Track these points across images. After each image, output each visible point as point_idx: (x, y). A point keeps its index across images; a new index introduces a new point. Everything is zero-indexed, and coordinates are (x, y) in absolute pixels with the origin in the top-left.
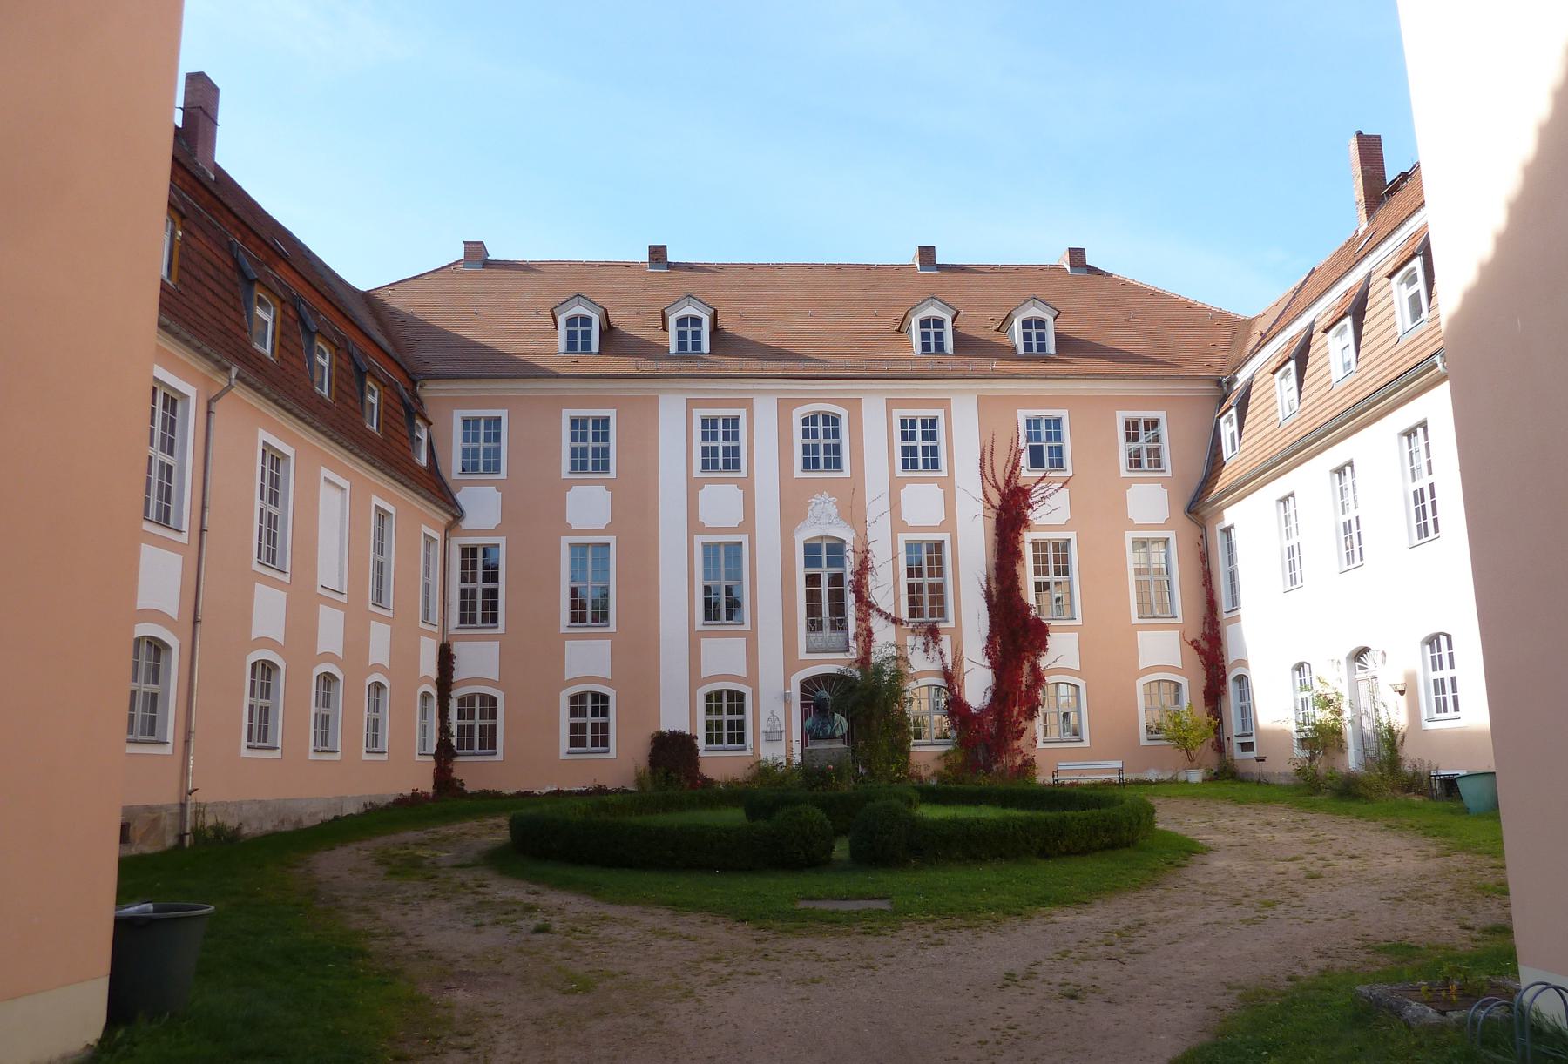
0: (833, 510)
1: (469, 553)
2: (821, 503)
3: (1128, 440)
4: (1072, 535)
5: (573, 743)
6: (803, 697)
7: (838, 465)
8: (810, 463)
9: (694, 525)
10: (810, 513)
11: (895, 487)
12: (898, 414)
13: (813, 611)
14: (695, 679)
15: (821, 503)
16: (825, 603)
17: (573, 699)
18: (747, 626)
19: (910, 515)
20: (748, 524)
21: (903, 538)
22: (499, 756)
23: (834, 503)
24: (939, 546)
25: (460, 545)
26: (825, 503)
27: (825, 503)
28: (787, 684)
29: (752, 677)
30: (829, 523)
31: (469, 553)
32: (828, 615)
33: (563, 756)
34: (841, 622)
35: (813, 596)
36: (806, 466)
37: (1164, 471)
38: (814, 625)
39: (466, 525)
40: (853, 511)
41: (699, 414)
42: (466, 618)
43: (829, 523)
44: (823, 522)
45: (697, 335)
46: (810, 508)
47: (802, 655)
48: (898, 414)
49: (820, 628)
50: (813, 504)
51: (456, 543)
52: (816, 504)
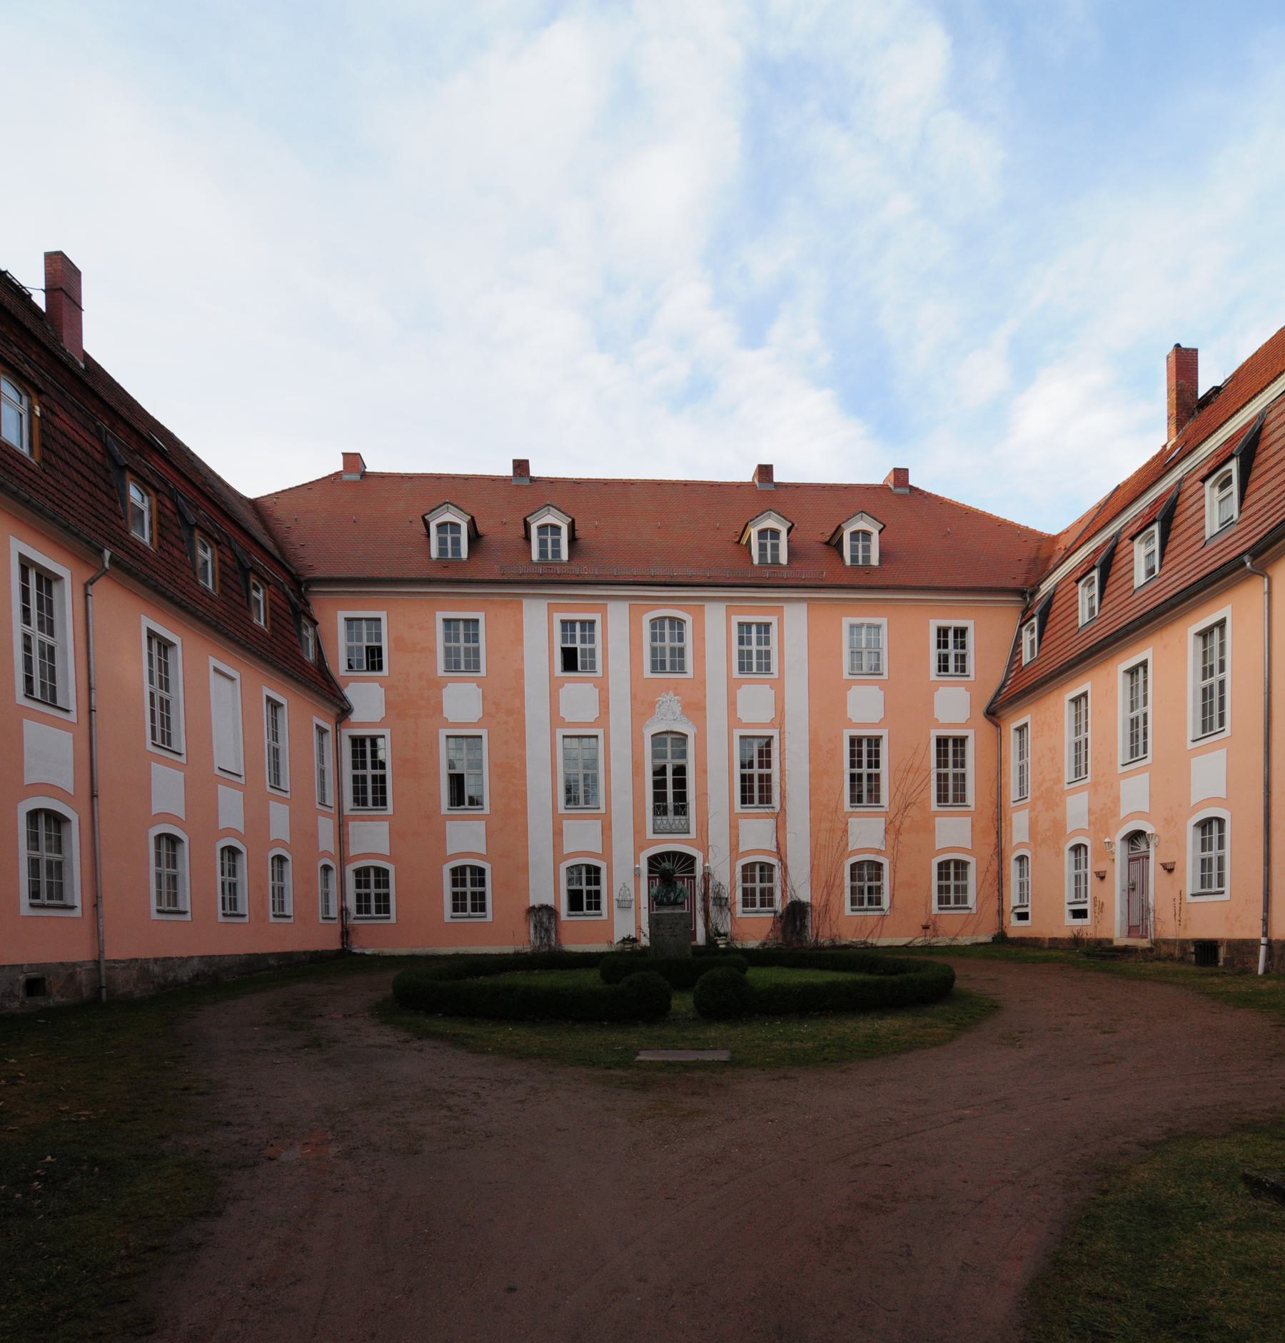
0: (678, 709)
1: (358, 742)
2: (667, 701)
3: (939, 647)
4: (883, 732)
5: (455, 909)
6: (650, 872)
7: (681, 668)
8: (658, 666)
9: (556, 720)
10: (657, 710)
11: (733, 686)
12: (736, 619)
13: (659, 797)
14: (558, 855)
15: (667, 701)
16: (670, 790)
17: (454, 871)
18: (603, 810)
19: (744, 714)
20: (603, 719)
21: (738, 733)
22: (393, 920)
23: (679, 702)
24: (769, 741)
25: (350, 736)
26: (670, 701)
27: (670, 701)
28: (637, 860)
29: (607, 853)
30: (675, 720)
31: (358, 742)
32: (672, 801)
33: (447, 919)
34: (684, 807)
35: (659, 784)
36: (654, 669)
37: (968, 676)
38: (660, 810)
39: (355, 717)
40: (695, 709)
41: (558, 617)
42: (360, 799)
43: (675, 720)
44: (669, 717)
45: (556, 543)
46: (658, 705)
47: (650, 835)
48: (736, 619)
49: (665, 813)
50: (660, 702)
51: (346, 733)
52: (663, 702)
